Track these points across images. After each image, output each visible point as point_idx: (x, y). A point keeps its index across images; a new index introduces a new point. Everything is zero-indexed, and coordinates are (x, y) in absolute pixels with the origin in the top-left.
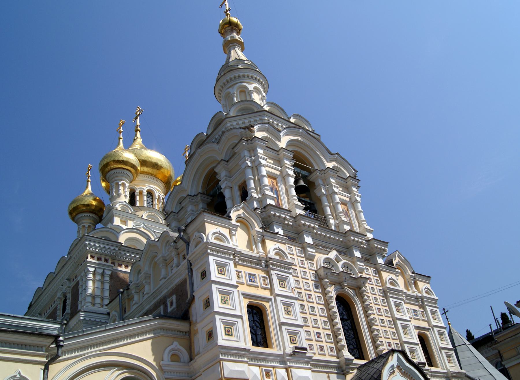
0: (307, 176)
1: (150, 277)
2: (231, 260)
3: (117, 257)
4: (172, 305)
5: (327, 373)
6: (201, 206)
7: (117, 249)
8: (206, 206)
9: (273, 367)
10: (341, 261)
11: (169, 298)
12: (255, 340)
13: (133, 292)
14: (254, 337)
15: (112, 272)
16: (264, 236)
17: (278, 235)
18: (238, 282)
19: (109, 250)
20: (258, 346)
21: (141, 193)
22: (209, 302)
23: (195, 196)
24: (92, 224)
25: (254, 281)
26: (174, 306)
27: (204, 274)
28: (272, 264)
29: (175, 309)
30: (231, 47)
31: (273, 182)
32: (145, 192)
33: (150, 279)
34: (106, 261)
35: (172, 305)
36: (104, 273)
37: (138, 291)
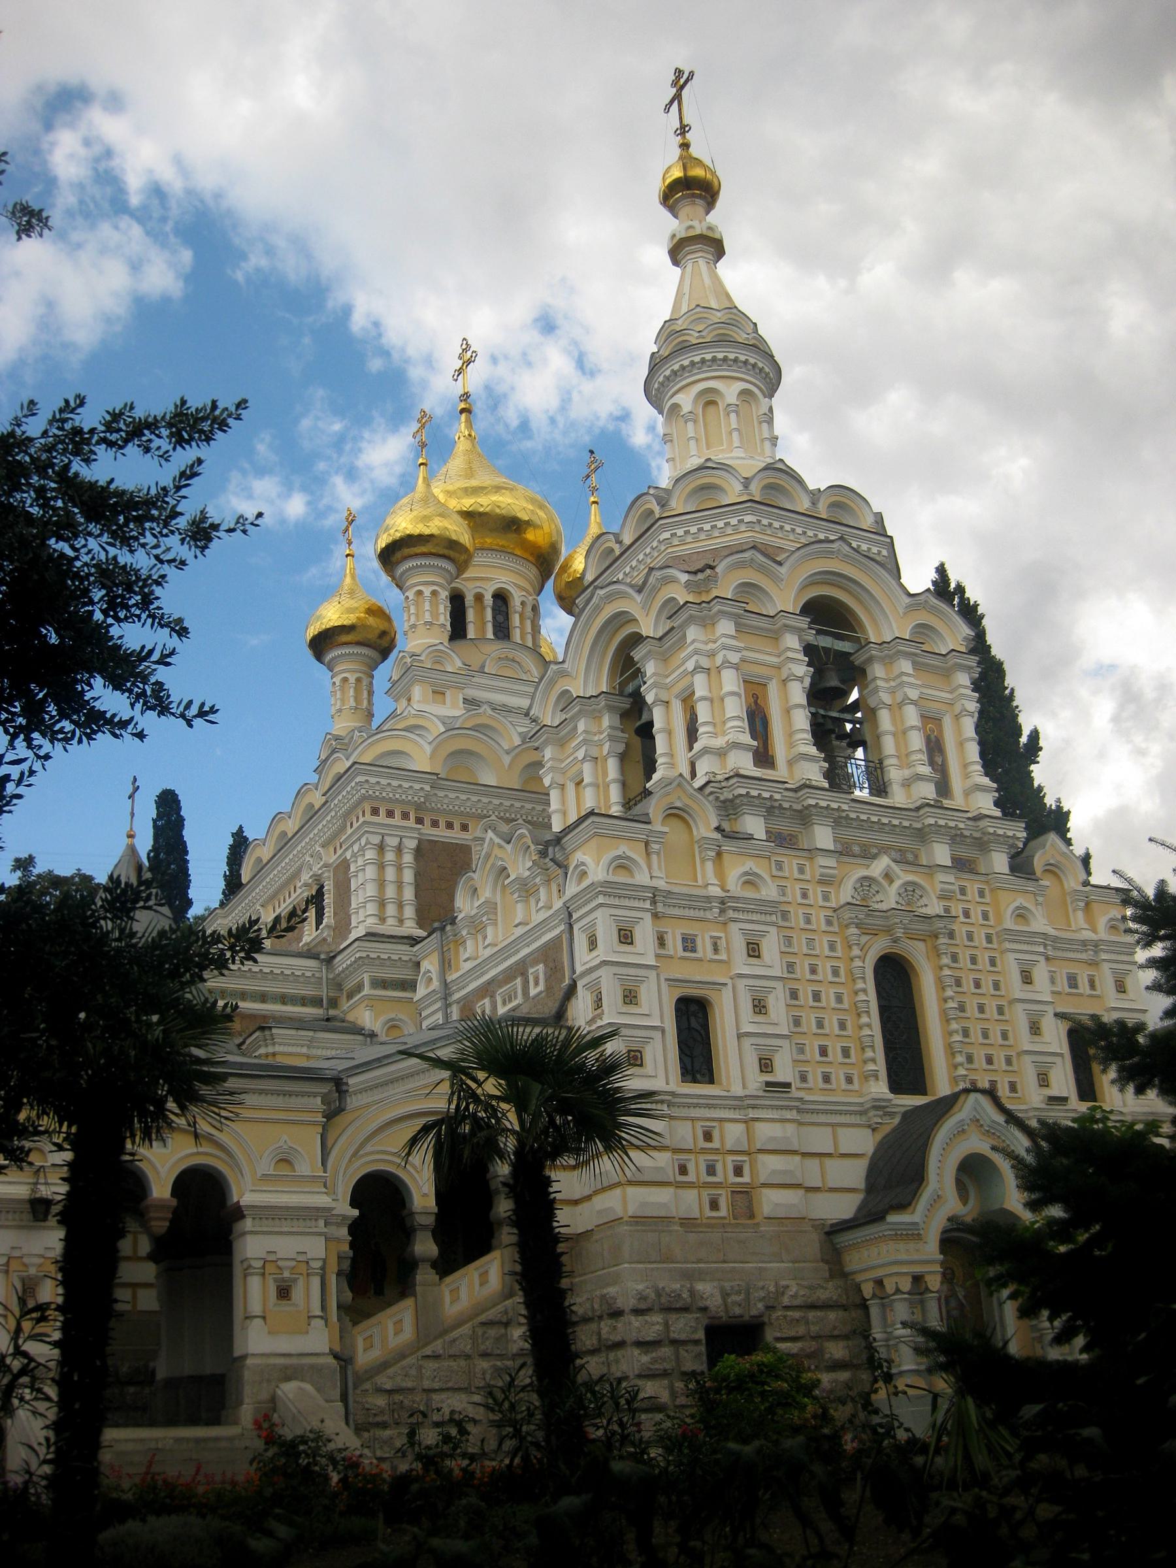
0: (850, 654)
1: (496, 909)
2: (647, 910)
3: (427, 804)
4: (537, 984)
5: (833, 1125)
6: (606, 721)
7: (427, 788)
8: (617, 722)
9: (721, 1120)
10: (899, 878)
11: (533, 967)
12: (689, 1068)
13: (464, 933)
14: (687, 1060)
15: (420, 841)
16: (720, 847)
17: (754, 842)
18: (657, 956)
19: (410, 792)
20: (695, 1081)
21: (479, 598)
22: (601, 999)
23: (592, 699)
24: (364, 673)
25: (694, 950)
26: (541, 987)
27: (593, 944)
28: (735, 909)
29: (543, 995)
30: (689, 257)
31: (758, 698)
32: (488, 600)
33: (496, 914)
34: (405, 816)
35: (537, 984)
36: (402, 846)
37: (474, 932)
